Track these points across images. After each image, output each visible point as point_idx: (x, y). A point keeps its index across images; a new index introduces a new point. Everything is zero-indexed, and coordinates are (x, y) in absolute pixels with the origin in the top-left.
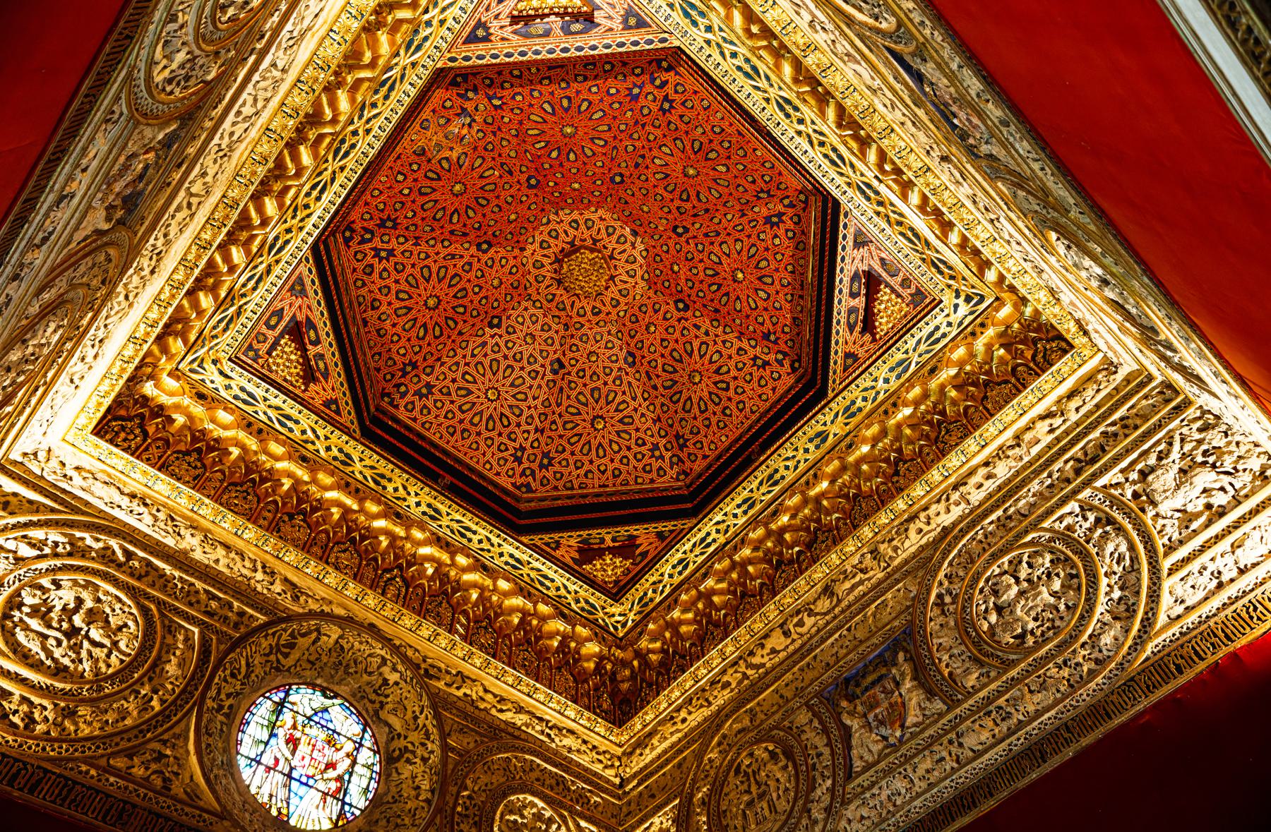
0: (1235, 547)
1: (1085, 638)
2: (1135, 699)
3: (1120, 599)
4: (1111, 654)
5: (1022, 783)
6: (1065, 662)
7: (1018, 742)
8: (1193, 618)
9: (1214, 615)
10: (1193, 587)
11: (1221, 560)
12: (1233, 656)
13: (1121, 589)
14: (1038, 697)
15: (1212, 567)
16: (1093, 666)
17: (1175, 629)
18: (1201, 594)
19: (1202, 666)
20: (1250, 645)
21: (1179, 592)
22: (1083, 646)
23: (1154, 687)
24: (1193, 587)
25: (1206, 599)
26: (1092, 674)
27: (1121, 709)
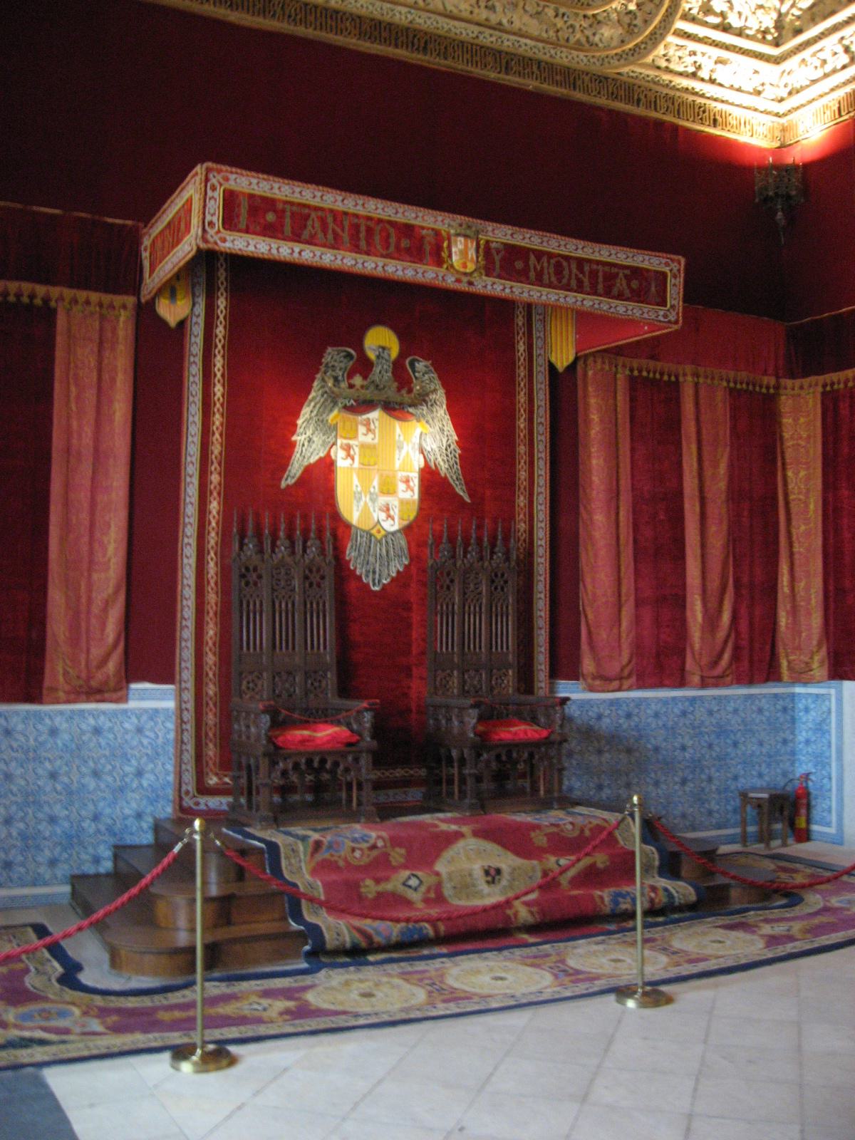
0: (720, 61)
1: (590, 13)
2: (599, 93)
3: (630, 12)
4: (600, 45)
5: (477, 72)
6: (564, 15)
7: (488, 39)
8: (666, 77)
9: (678, 89)
10: (680, 58)
11: (707, 57)
12: (675, 128)
13: (638, 5)
14: (526, 19)
15: (699, 58)
16: (583, 40)
17: (652, 73)
18: (680, 69)
19: (653, 114)
20: (687, 130)
21: (671, 52)
22: (585, 16)
23: (616, 97)
24: (680, 58)
25: (681, 74)
26: (578, 46)
27: (587, 91)
